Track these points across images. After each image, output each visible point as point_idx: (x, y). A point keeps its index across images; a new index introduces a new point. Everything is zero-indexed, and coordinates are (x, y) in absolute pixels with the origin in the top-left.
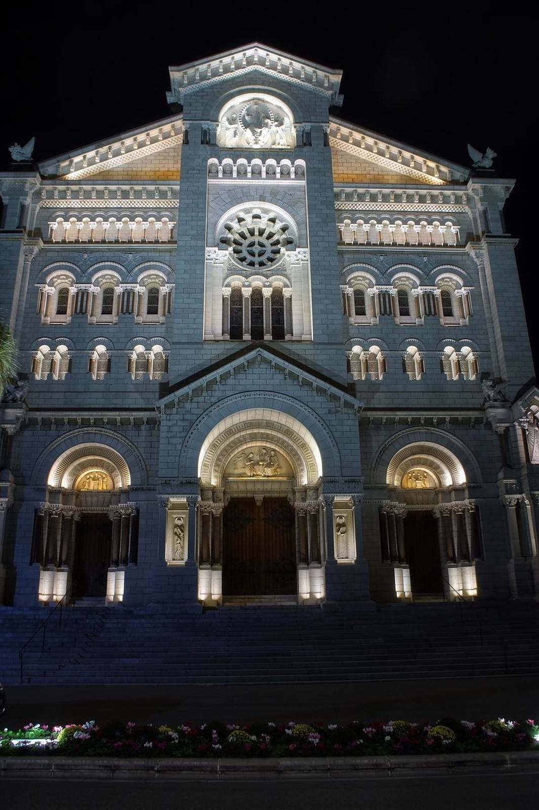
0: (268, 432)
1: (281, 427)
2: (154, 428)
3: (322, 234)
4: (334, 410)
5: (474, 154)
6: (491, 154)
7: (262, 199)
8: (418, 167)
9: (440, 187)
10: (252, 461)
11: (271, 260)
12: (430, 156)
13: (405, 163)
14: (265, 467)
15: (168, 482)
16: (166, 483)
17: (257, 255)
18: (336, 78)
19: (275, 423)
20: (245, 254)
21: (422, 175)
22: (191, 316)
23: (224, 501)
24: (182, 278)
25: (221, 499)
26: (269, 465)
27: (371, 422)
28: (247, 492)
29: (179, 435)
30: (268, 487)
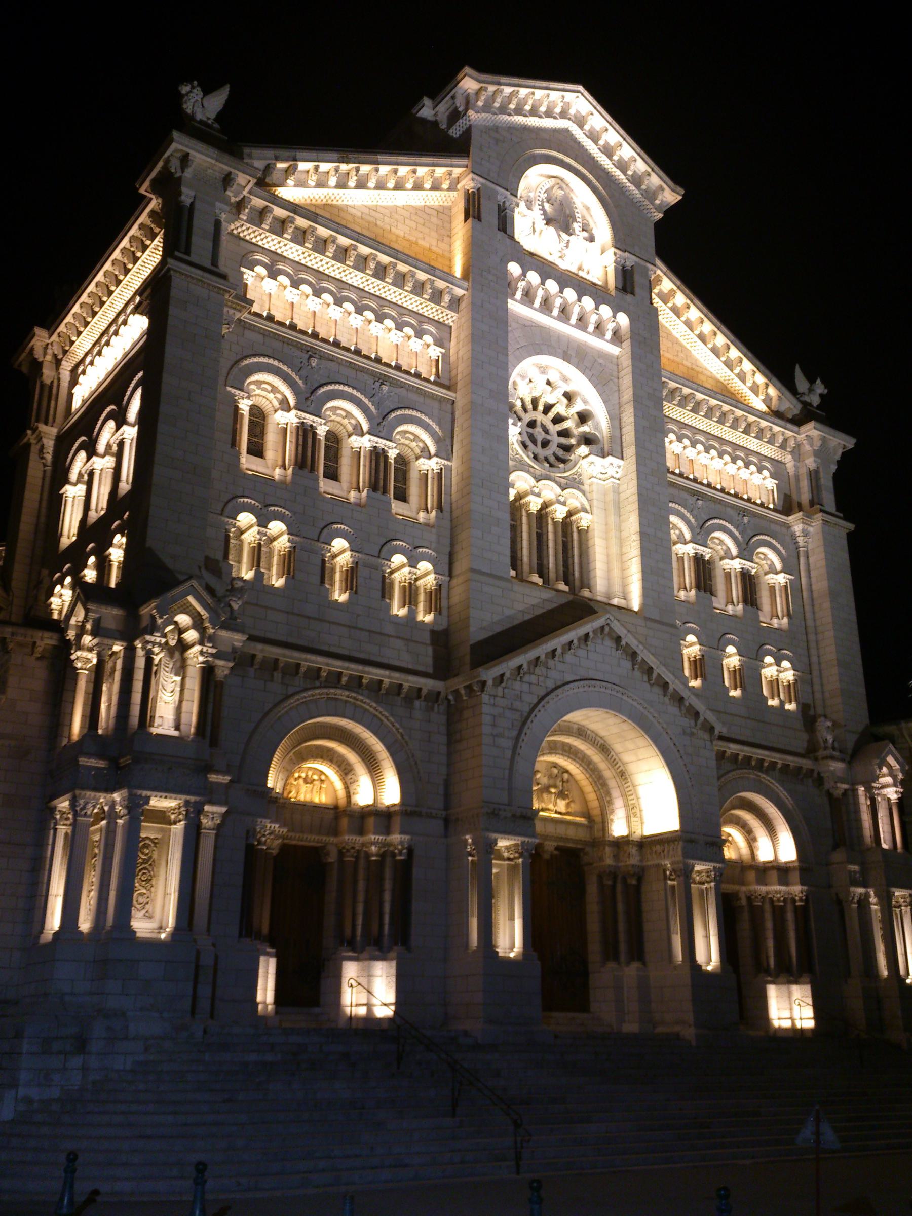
2: (432, 709)
5: (801, 383)
6: (820, 388)
7: (566, 357)
8: (742, 377)
9: (757, 413)
12: (762, 368)
13: (729, 364)
15: (496, 812)
16: (493, 813)
18: (670, 196)
21: (743, 389)
26: (561, 795)
30: (561, 831)
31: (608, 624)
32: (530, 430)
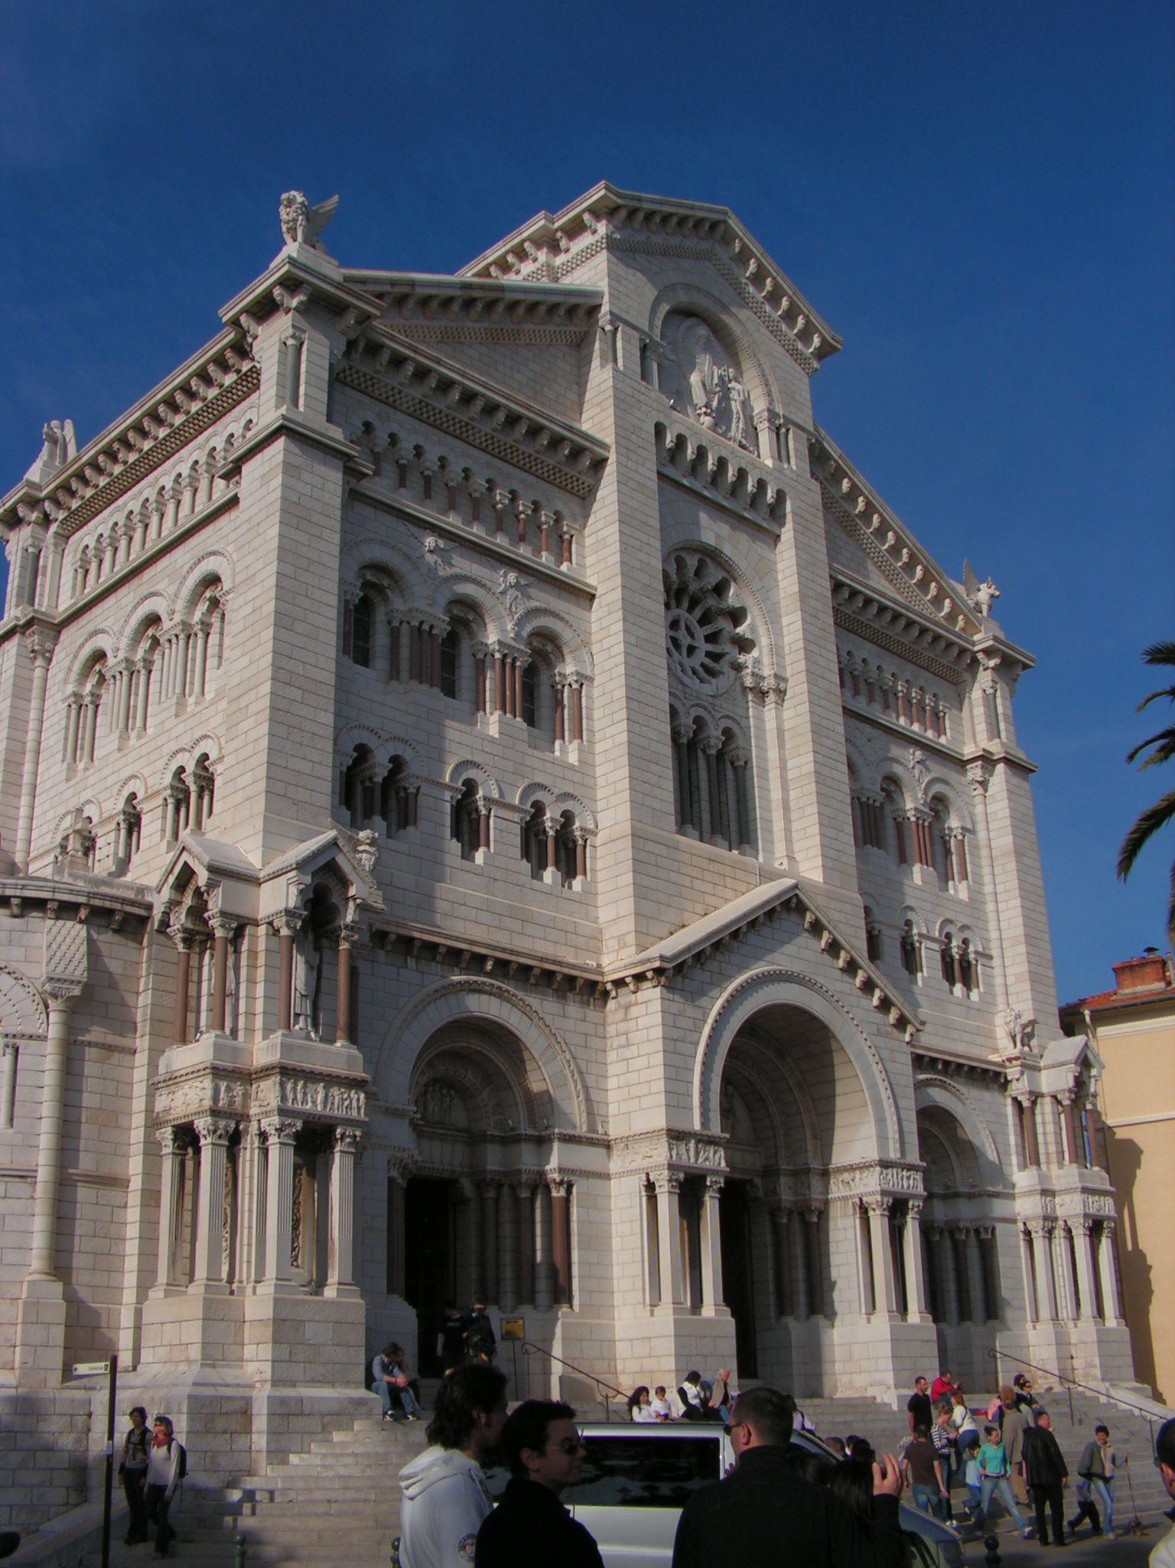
11: (711, 673)
32: (673, 634)
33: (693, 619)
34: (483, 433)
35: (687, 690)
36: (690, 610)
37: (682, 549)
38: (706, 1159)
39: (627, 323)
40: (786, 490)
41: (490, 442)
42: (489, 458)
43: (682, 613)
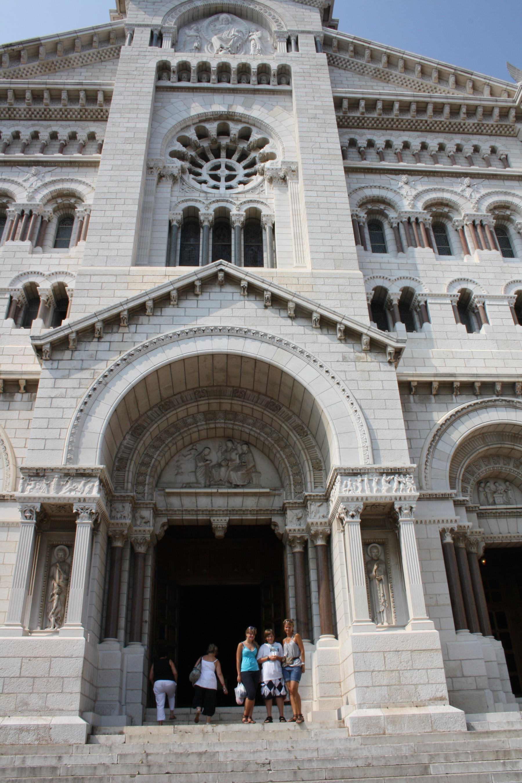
0: (237, 405)
1: (258, 398)
3: (318, 140)
4: (352, 356)
10: (207, 460)
14: (232, 470)
17: (223, 179)
19: (249, 392)
20: (205, 176)
22: (113, 232)
23: (154, 526)
24: (105, 186)
25: (149, 522)
27: (414, 389)
28: (197, 512)
29: (70, 393)
31: (221, 270)
33: (233, 162)
34: (22, 110)
35: (208, 195)
36: (229, 156)
37: (200, 121)
38: (71, 491)
39: (139, 26)
40: (288, 63)
41: (30, 113)
42: (36, 122)
43: (223, 160)
